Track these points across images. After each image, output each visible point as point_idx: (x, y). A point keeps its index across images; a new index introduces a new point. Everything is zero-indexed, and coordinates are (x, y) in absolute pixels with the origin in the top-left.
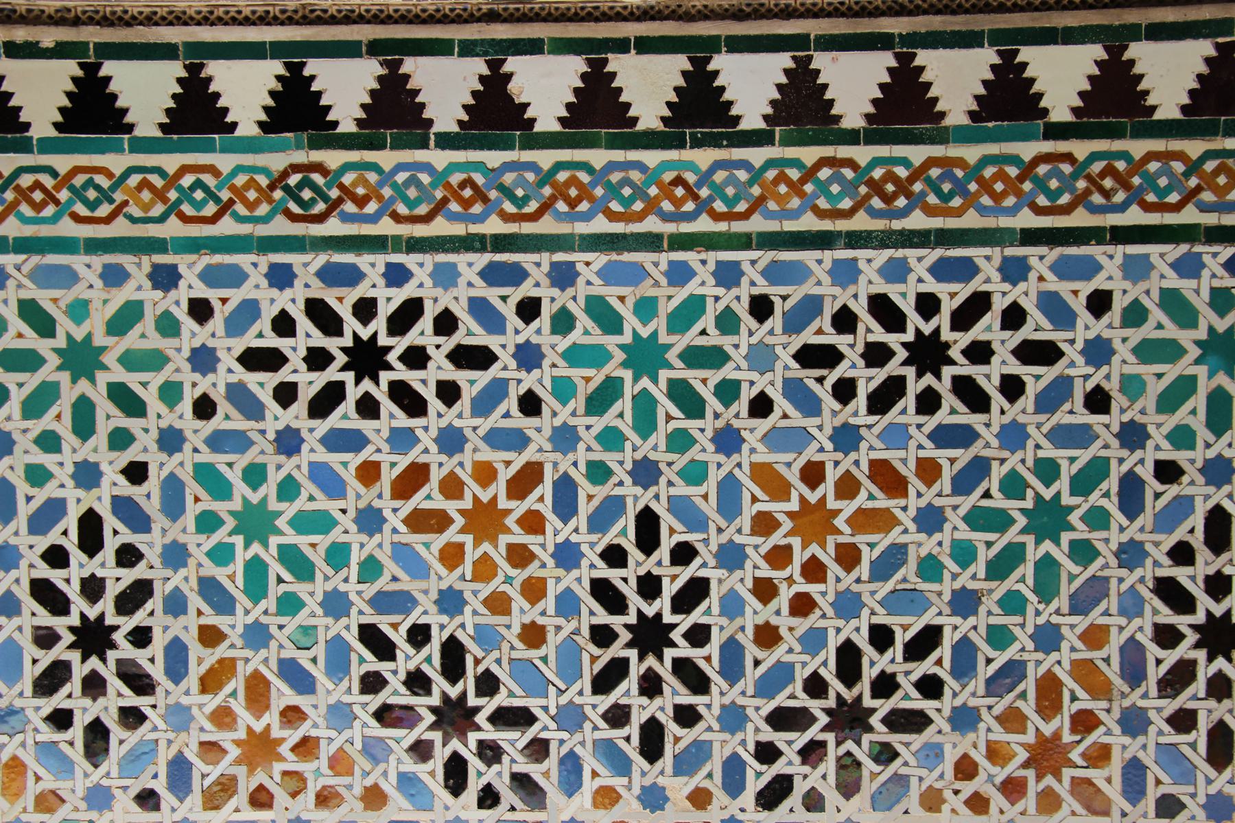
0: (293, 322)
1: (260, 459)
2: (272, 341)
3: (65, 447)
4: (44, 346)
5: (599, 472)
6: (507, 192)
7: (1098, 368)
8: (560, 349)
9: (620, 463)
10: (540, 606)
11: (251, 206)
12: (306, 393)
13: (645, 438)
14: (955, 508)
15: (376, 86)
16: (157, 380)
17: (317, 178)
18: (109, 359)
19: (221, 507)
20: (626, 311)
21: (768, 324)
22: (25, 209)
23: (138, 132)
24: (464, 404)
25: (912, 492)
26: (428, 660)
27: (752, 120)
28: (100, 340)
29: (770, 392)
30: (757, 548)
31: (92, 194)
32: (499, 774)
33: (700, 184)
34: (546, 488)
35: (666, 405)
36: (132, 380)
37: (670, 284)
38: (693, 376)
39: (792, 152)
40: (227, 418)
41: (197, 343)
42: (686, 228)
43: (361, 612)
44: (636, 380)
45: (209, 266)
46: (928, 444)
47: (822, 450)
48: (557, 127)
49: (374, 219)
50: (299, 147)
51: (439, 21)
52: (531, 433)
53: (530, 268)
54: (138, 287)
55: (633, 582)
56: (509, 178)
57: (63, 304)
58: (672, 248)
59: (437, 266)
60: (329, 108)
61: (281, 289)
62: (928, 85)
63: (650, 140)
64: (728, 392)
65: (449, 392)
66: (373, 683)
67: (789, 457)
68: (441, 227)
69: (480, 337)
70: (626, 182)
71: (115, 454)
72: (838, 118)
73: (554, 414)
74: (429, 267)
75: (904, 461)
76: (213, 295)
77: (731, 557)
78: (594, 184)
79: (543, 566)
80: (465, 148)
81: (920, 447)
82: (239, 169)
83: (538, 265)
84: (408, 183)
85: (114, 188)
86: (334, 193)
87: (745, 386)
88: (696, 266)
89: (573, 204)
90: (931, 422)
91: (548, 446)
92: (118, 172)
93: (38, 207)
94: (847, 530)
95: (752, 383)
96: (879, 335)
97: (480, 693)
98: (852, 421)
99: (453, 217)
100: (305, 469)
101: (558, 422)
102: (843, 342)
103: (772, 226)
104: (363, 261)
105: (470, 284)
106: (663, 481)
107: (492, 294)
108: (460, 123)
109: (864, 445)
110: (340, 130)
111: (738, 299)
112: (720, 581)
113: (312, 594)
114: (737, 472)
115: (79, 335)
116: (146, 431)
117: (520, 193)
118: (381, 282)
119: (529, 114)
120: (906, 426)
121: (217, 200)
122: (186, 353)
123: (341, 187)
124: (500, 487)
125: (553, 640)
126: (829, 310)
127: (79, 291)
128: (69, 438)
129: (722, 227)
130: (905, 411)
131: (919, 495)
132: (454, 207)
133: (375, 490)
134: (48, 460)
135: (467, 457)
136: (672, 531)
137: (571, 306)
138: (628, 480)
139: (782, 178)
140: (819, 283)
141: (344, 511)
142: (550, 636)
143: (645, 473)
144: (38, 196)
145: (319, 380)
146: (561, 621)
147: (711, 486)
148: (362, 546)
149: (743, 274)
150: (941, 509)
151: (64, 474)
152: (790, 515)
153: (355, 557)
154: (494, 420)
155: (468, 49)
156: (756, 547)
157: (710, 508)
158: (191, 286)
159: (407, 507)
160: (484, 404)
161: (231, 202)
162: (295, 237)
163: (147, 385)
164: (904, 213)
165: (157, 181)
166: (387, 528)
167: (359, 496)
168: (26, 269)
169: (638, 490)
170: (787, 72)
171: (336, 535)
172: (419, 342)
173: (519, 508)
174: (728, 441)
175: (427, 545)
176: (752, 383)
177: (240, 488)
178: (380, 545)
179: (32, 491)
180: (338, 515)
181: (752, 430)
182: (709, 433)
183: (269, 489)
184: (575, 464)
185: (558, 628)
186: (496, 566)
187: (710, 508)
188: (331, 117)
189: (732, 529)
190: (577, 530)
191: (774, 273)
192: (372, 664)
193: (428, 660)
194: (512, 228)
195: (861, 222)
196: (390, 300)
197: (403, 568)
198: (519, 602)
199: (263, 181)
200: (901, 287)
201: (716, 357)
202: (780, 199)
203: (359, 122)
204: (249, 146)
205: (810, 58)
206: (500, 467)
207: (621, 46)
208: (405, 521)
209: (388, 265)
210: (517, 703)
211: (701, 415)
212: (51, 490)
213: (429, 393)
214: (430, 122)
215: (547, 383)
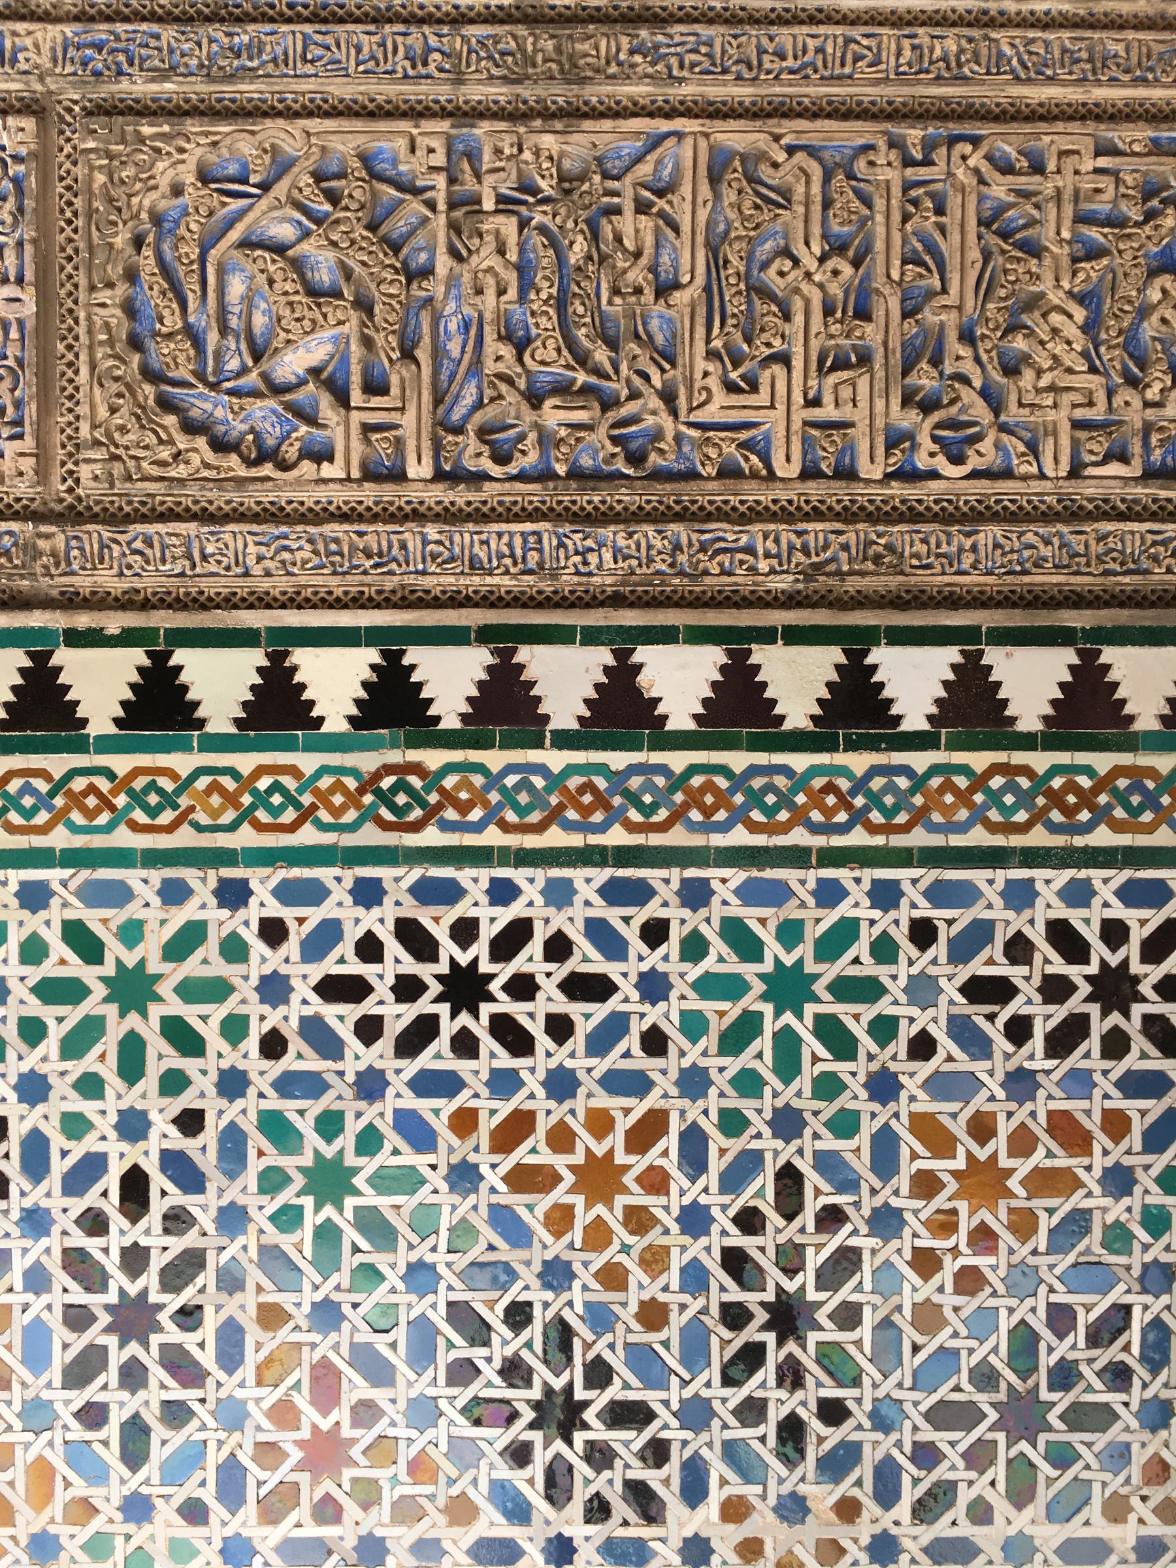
0: (380, 945)
1: (337, 1106)
2: (355, 967)
3: (109, 1093)
4: (89, 974)
5: (733, 1123)
6: (633, 799)
8: (690, 978)
9: (758, 1112)
11: (337, 812)
12: (393, 1028)
13: (787, 1082)
14: (1147, 1168)
15: (484, 676)
16: (218, 1013)
17: (415, 781)
18: (165, 989)
19: (288, 1162)
20: (767, 936)
21: (931, 952)
22: (77, 817)
23: (209, 728)
24: (578, 1041)
25: (1097, 1149)
26: (529, 1345)
27: (915, 721)
28: (155, 966)
29: (932, 1029)
30: (917, 1214)
31: (153, 799)
32: (610, 1482)
33: (853, 792)
34: (671, 1141)
35: (812, 1044)
36: (190, 1013)
37: (819, 905)
38: (843, 1011)
39: (959, 757)
40: (300, 1058)
41: (267, 970)
42: (837, 841)
43: (450, 1288)
44: (778, 1014)
45: (284, 881)
46: (1115, 1092)
47: (992, 1098)
48: (691, 725)
49: (478, 827)
50: (394, 745)
51: (557, 605)
52: (655, 1076)
53: (657, 885)
54: (201, 904)
55: (771, 1251)
56: (635, 782)
57: (113, 926)
58: (821, 864)
59: (550, 882)
60: (430, 701)
61: (368, 907)
62: (1115, 685)
63: (798, 742)
64: (884, 1029)
65: (560, 1028)
66: (463, 1372)
67: (954, 1107)
68: (555, 837)
69: (598, 964)
70: (770, 788)
71: (166, 1101)
72: (1013, 720)
73: (683, 1054)
74: (540, 883)
75: (1088, 1112)
76: (288, 914)
77: (886, 1222)
78: (732, 791)
79: (667, 1232)
80: (586, 748)
81: (1106, 1096)
82: (324, 770)
83: (667, 881)
84: (518, 787)
85: (179, 792)
86: (433, 798)
87: (903, 1023)
88: (850, 885)
89: (708, 812)
90: (1119, 1069)
91: (674, 1091)
92: (184, 774)
93: (91, 814)
94: (1021, 1192)
95: (912, 1020)
96: (1059, 966)
97: (589, 1384)
98: (1027, 1065)
99: (569, 826)
100: (389, 1117)
101: (686, 1063)
102: (1017, 973)
103: (936, 840)
104: (463, 876)
105: (587, 903)
106: (808, 1132)
107: (613, 915)
108: (581, 719)
109: (1041, 1094)
110: (442, 726)
112: (874, 1252)
113: (393, 1266)
114: (893, 1123)
115: (130, 960)
116: (204, 1072)
117: (647, 799)
118: (484, 899)
119: (661, 710)
120: (1090, 1072)
121: (297, 805)
122: (254, 981)
123: (442, 791)
124: (617, 1139)
125: (677, 1320)
126: (1001, 937)
127: (133, 910)
128: (113, 1081)
129: (879, 840)
130: (1088, 1055)
131: (1104, 1154)
132: (572, 815)
133: (471, 1142)
134: (89, 1108)
135: (580, 1103)
136: (818, 1192)
137: (704, 929)
138: (767, 1132)
139: (948, 786)
140: (990, 906)
141: (434, 1167)
142: (674, 1316)
143: (787, 1123)
144: (91, 801)
145: (408, 1013)
146: (686, 1298)
147: (863, 1139)
148: (454, 1208)
149: (902, 894)
150: (1131, 1169)
151: (106, 1125)
152: (955, 1174)
154: (612, 1060)
155: (592, 637)
156: (916, 1212)
157: (862, 1164)
158: (265, 902)
159: (508, 1163)
160: (600, 1043)
161: (314, 807)
162: (386, 848)
163: (206, 1021)
164: (1088, 828)
165: (229, 783)
166: (483, 1187)
167: (451, 1150)
168: (73, 885)
169: (779, 1144)
170: (954, 667)
172: (527, 968)
173: (640, 1164)
174: (884, 1087)
175: (530, 1208)
176: (912, 1020)
177: (312, 1139)
178: (475, 1208)
179: (67, 1145)
180: (427, 1172)
181: (912, 1075)
182: (862, 1078)
183: (347, 1141)
184: (705, 1112)
185: (683, 1307)
186: (611, 1232)
187: (862, 1164)
188: (432, 711)
189: (888, 1190)
190: (705, 1190)
191: (938, 894)
193: (529, 1345)
194: (638, 839)
195: (1038, 837)
196: (494, 921)
198: (637, 1275)
199: (351, 783)
200: (1083, 912)
201: (869, 990)
202: (946, 810)
203: (464, 717)
204: (336, 743)
205: (981, 653)
206: (618, 1115)
207: (767, 636)
209: (493, 880)
210: (632, 1396)
211: (853, 1057)
212: (90, 1144)
213: (536, 1029)
214: (546, 718)
215: (675, 1017)
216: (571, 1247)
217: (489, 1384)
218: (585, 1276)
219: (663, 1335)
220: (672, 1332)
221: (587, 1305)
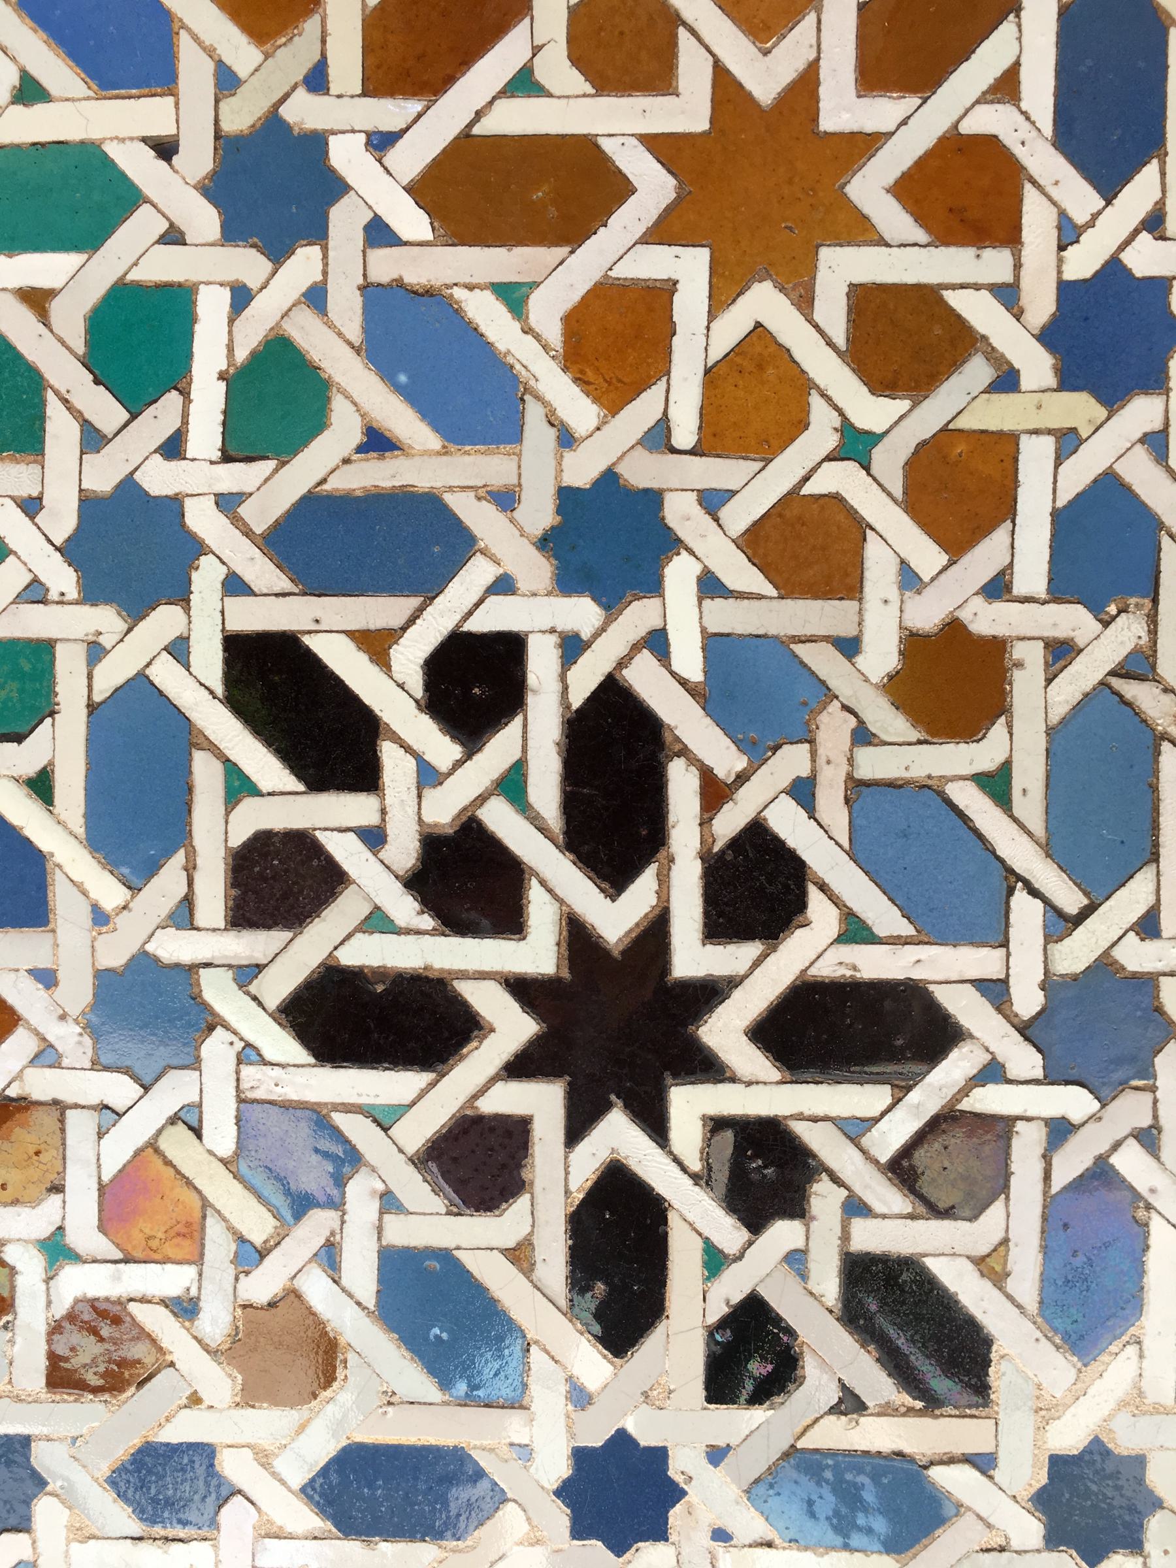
10: (986, 557)
26: (512, 784)
32: (796, 1260)
43: (234, 585)
66: (281, 881)
79: (1007, 380)
97: (721, 925)
125: (1037, 701)
141: (165, 149)
142: (1026, 685)
146: (1072, 619)
148: (241, 297)
153: (212, 350)
166: (345, 221)
167: (227, 82)
171: (131, 253)
175: (513, 296)
178: (316, 297)
180: (138, 164)
185: (1061, 652)
192: (284, 802)
193: (512, 784)
197: (410, 395)
198: (896, 537)
208: (425, 190)
210: (875, 964)
216: (659, 438)
217: (377, 921)
218: (709, 545)
219: (986, 753)
220: (1021, 740)
221: (715, 644)
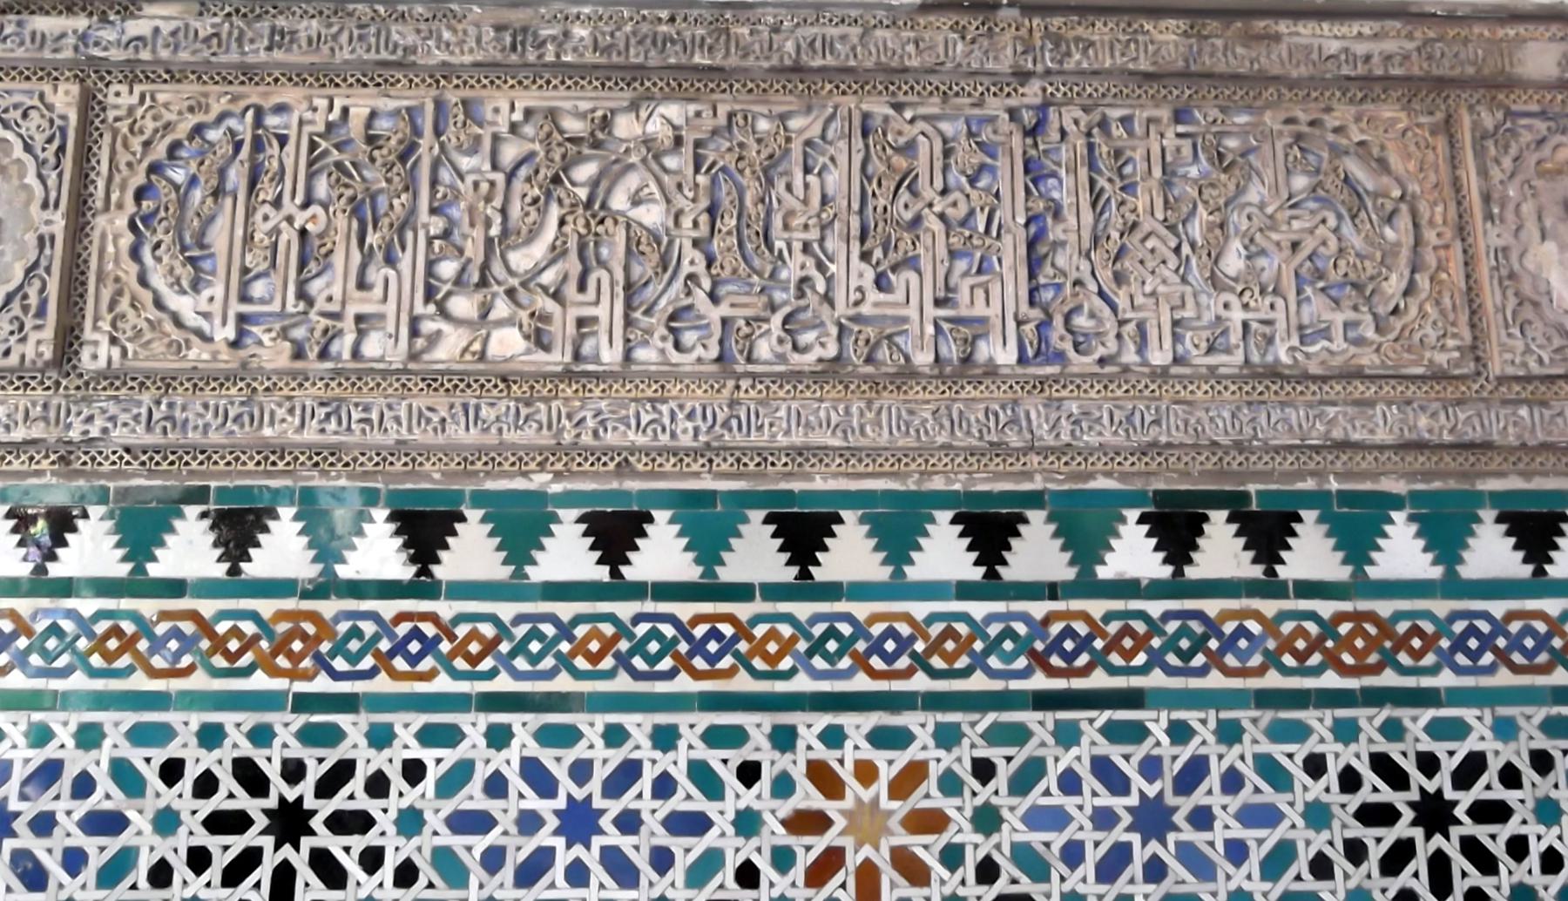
7: (1330, 828)
111: (960, 760)
